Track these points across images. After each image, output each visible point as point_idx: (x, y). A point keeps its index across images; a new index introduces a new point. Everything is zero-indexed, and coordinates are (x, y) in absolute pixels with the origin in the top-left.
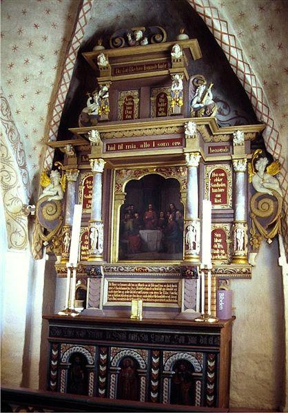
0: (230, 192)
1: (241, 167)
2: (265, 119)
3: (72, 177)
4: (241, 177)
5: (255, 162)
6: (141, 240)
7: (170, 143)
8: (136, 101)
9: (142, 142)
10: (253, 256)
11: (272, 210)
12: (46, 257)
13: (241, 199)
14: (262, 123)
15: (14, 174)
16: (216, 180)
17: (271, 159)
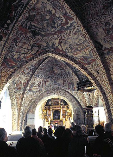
1: (66, 110)
3: (47, 110)
4: (66, 111)
7: (59, 107)
13: (66, 113)
17: (69, 109)
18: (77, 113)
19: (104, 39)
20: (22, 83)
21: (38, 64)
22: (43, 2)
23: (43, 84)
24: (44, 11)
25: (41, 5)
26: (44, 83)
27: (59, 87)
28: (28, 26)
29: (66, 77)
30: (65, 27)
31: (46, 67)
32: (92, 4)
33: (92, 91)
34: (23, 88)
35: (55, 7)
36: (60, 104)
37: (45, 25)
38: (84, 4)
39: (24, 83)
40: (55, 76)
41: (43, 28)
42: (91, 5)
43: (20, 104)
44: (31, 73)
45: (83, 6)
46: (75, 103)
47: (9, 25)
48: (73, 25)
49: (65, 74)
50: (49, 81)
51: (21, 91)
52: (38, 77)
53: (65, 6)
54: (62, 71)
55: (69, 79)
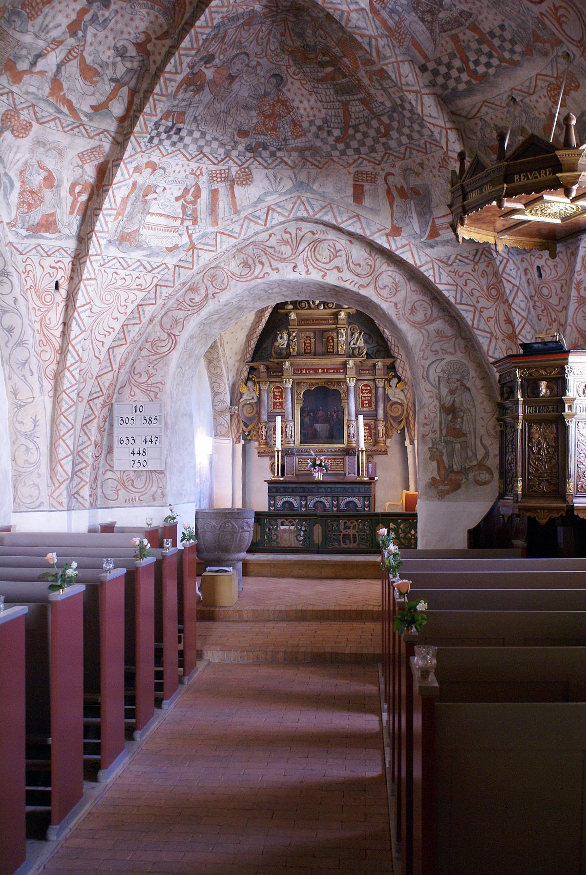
0: (373, 400)
1: (380, 384)
2: (396, 355)
4: (380, 390)
5: (390, 381)
6: (316, 430)
7: (336, 370)
8: (313, 340)
9: (318, 369)
10: (389, 440)
11: (400, 412)
12: (243, 442)
14: (394, 357)
15: (223, 385)
16: (365, 391)
17: (400, 379)
18: (448, 400)
20: (61, 181)
21: (165, 35)
23: (214, 193)
26: (222, 188)
27: (328, 218)
29: (372, 149)
31: (234, 71)
33: (559, 247)
34: (69, 225)
36: (342, 348)
39: (78, 189)
40: (299, 142)
43: (58, 333)
44: (118, 108)
46: (438, 332)
49: (368, 125)
50: (259, 174)
51: (59, 243)
52: (174, 144)
54: (346, 104)
55: (398, 164)
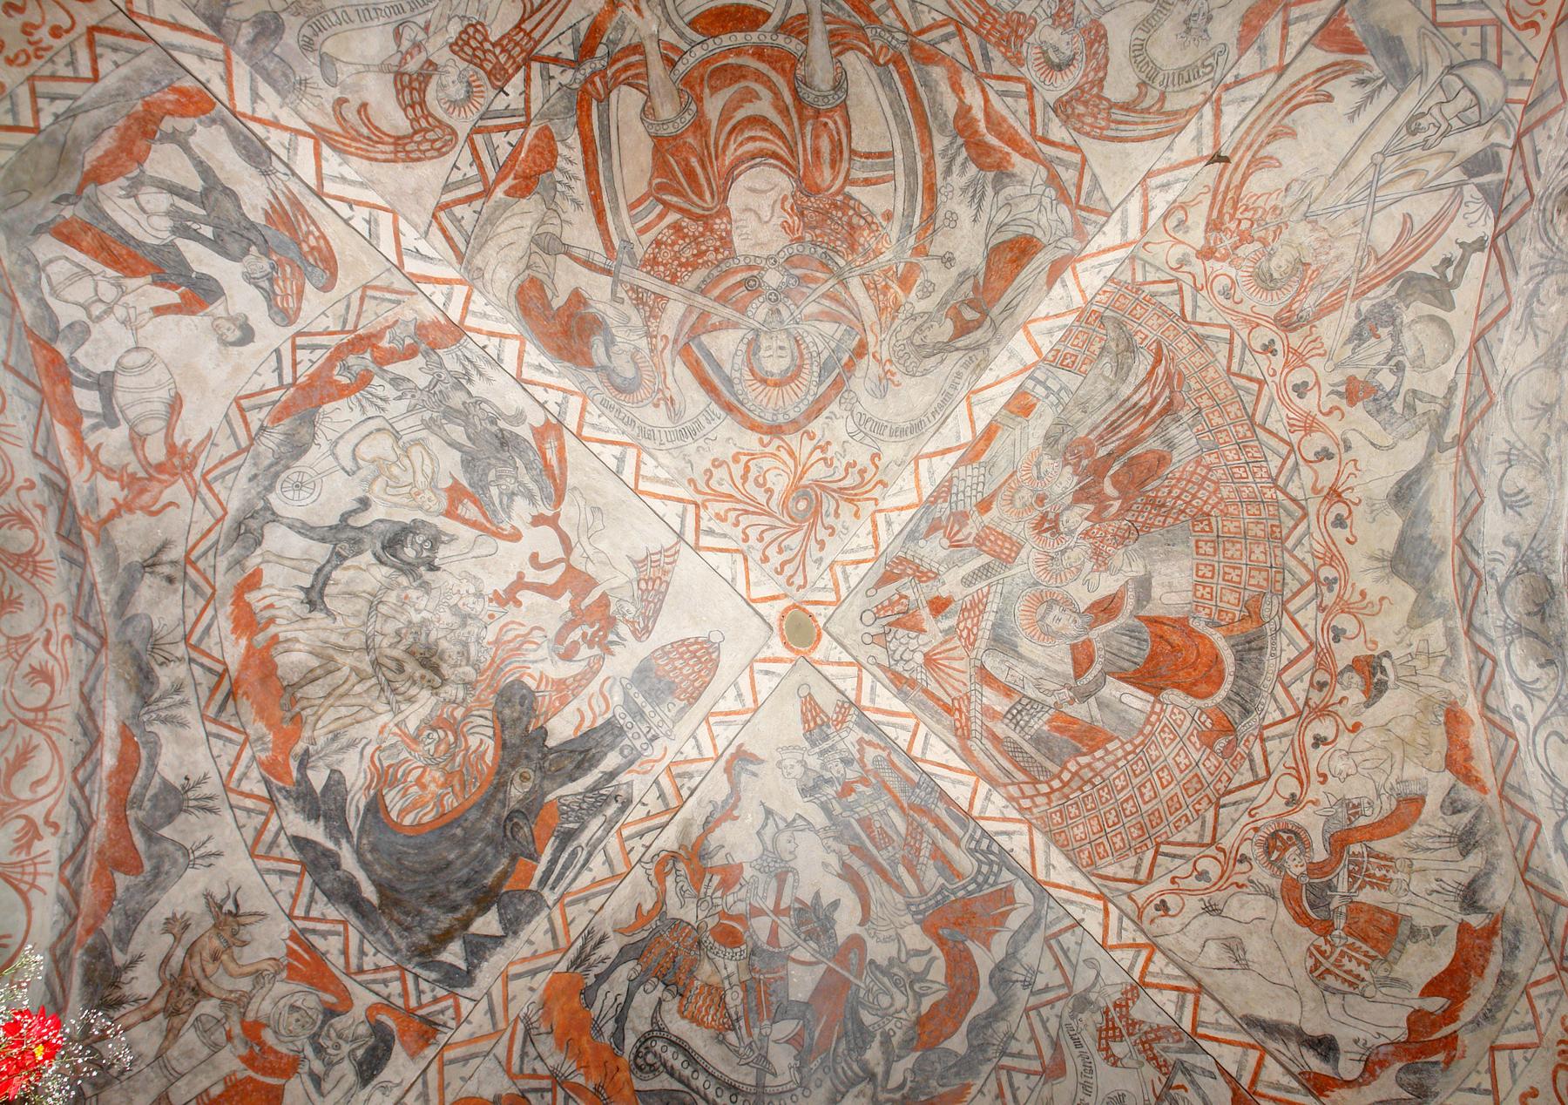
19: (1318, 973)
22: (769, 813)
24: (777, 903)
25: (758, 833)
28: (633, 1029)
30: (947, 1044)
32: (1120, 753)
35: (856, 863)
37: (782, 1058)
38: (1064, 767)
41: (760, 1085)
42: (1114, 763)
45: (1059, 776)
47: (478, 949)
48: (1019, 973)
53: (932, 763)
